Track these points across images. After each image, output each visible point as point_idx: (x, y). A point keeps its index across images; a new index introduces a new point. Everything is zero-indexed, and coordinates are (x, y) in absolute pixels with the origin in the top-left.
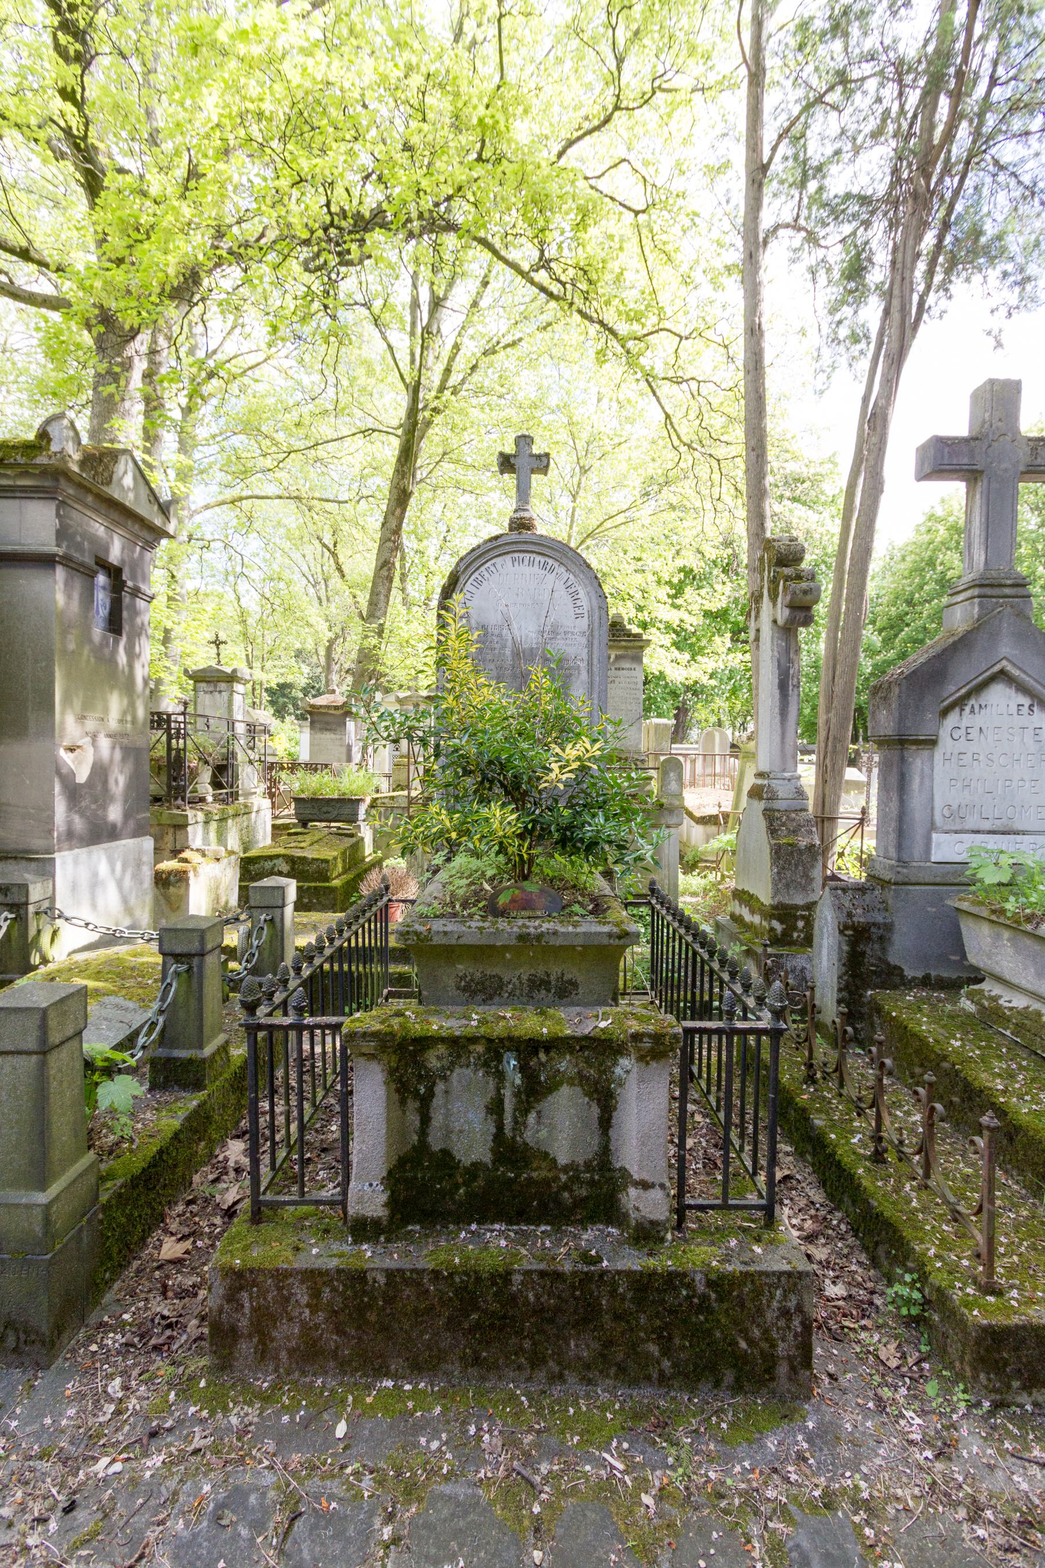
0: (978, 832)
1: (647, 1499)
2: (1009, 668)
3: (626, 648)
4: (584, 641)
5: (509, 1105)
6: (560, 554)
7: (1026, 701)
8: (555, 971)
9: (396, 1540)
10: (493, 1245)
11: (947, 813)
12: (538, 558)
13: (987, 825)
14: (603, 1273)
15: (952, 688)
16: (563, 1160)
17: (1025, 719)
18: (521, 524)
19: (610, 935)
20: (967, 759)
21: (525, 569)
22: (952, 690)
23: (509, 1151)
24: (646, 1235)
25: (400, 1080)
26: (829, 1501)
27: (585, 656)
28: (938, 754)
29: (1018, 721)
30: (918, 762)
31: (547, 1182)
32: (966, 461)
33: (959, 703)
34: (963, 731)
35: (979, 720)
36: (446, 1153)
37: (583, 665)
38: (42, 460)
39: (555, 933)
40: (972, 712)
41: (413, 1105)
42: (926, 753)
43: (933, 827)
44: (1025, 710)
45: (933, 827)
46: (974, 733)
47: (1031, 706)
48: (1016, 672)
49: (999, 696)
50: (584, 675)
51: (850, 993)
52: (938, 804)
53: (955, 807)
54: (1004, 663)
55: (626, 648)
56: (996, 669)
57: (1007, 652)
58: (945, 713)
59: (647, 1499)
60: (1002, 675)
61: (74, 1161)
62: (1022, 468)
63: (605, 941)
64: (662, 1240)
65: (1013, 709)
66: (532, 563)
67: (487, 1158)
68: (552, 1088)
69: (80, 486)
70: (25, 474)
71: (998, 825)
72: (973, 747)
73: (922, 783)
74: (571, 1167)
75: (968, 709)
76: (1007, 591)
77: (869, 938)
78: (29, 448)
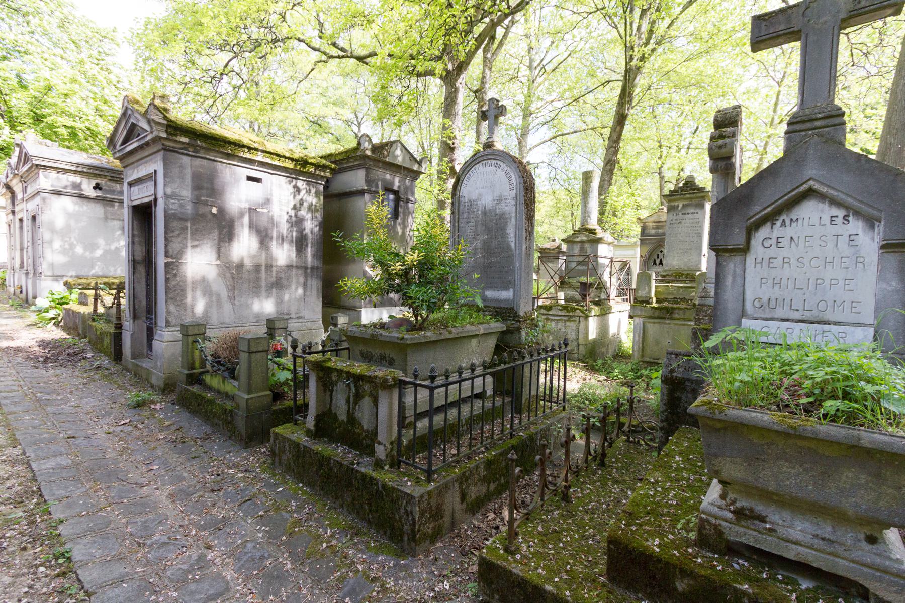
0: (788, 320)
1: (325, 545)
2: (816, 186)
3: (691, 199)
4: (513, 202)
5: (352, 399)
6: (504, 156)
7: (841, 213)
8: (387, 352)
9: (261, 516)
10: (337, 452)
11: (757, 304)
12: (494, 162)
13: (797, 315)
14: (353, 469)
15: (758, 208)
16: (365, 428)
17: (840, 227)
18: (489, 145)
19: (398, 338)
20: (778, 262)
21: (488, 169)
22: (758, 209)
23: (352, 420)
24: (378, 465)
25: (323, 382)
26: (374, 580)
27: (514, 211)
28: (750, 260)
29: (831, 230)
30: (731, 266)
31: (359, 435)
32: (782, 27)
33: (770, 218)
34: (774, 241)
35: (789, 231)
36: (335, 414)
37: (513, 216)
38: (359, 153)
39: (381, 335)
40: (783, 224)
41: (328, 393)
42: (738, 259)
43: (743, 314)
44: (840, 220)
45: (743, 314)
46: (785, 242)
47: (845, 217)
48: (823, 189)
49: (810, 211)
50: (513, 220)
51: (669, 424)
52: (749, 296)
53: (765, 299)
54: (811, 183)
55: (691, 199)
56: (805, 187)
57: (813, 173)
58: (758, 225)
59: (325, 545)
60: (810, 194)
61: (263, 391)
62: (843, 15)
63: (396, 341)
64: (383, 468)
65: (826, 219)
66: (491, 165)
67: (345, 420)
68: (363, 397)
69: (375, 160)
70: (356, 160)
71: (808, 315)
72: (784, 253)
73: (734, 281)
74: (367, 431)
75: (779, 223)
76: (818, 123)
77: (684, 389)
78: (355, 149)
